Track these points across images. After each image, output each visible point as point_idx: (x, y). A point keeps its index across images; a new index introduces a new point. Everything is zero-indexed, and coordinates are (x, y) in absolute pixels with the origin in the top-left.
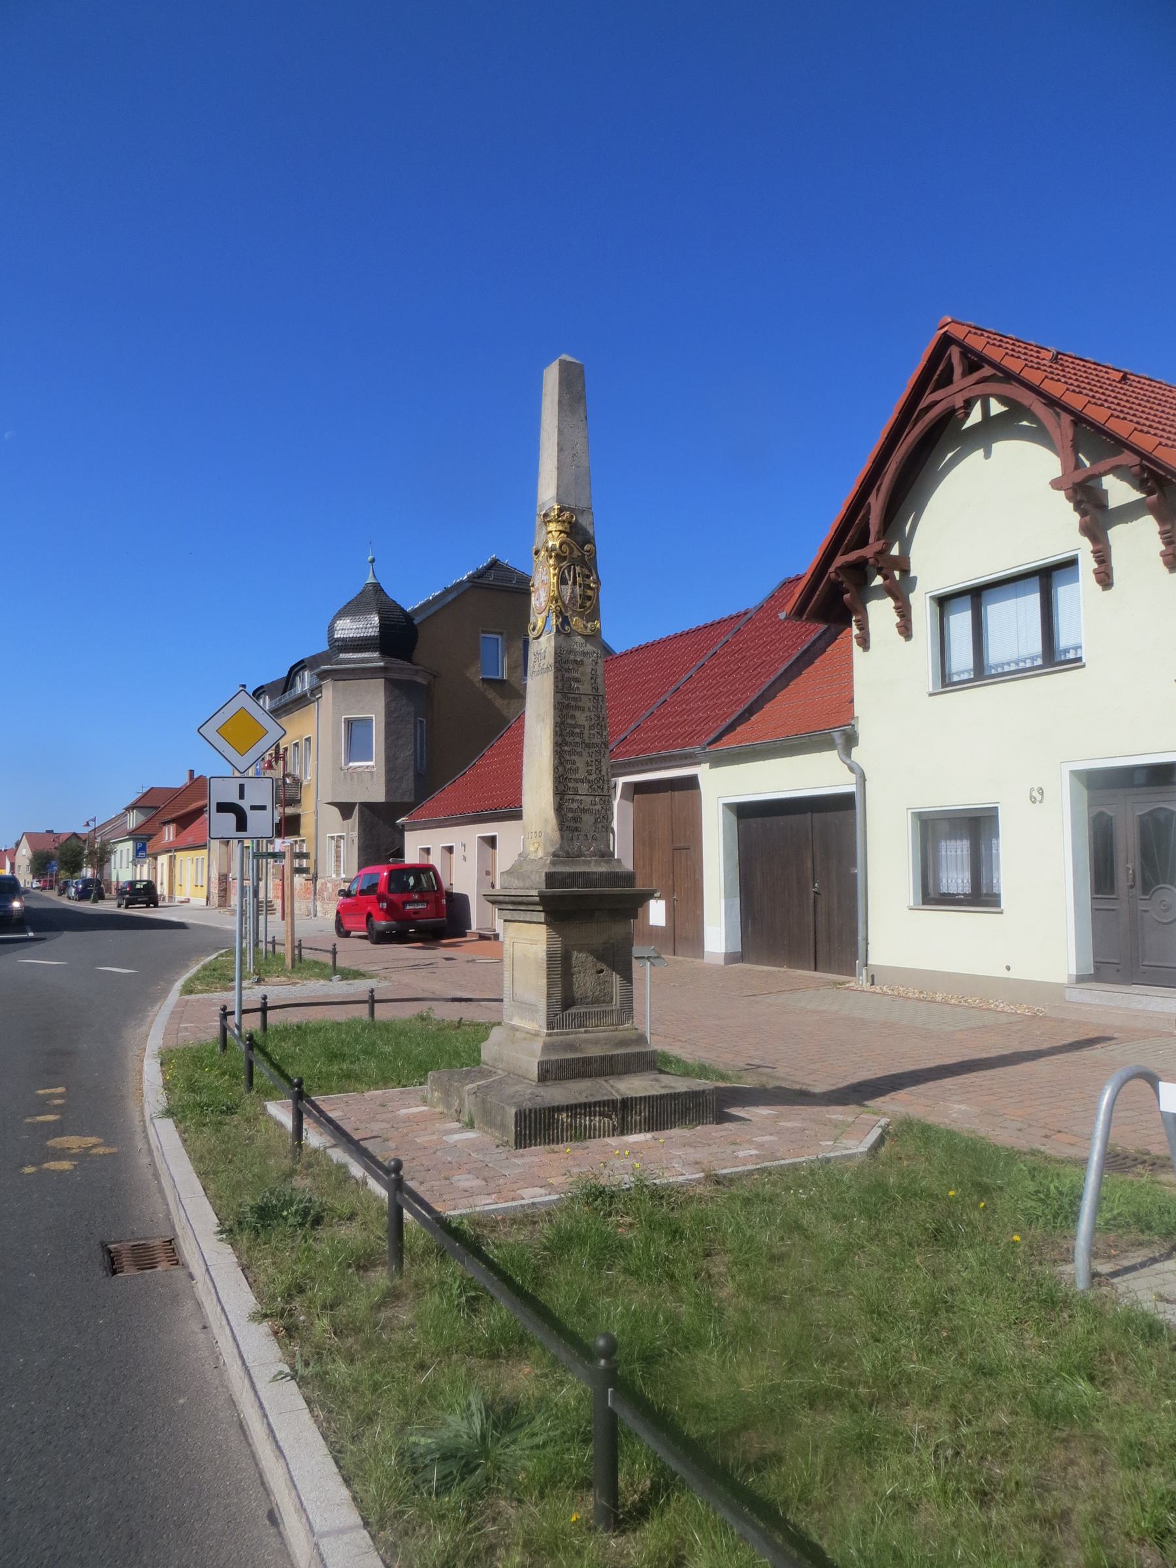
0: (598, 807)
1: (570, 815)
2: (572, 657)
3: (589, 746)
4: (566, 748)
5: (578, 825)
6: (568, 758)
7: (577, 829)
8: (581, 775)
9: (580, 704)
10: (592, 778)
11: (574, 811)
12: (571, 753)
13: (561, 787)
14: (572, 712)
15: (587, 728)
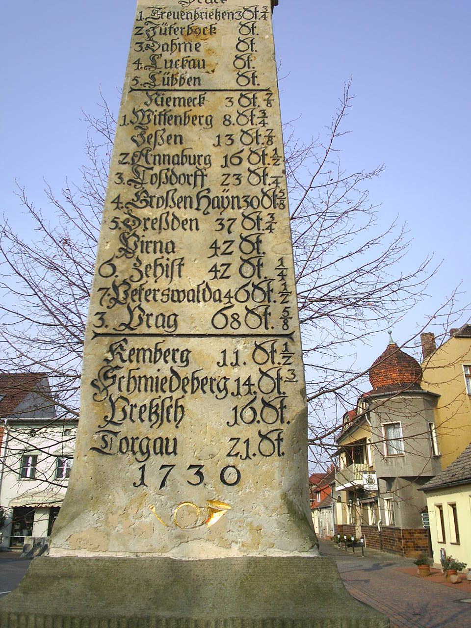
0: (250, 371)
1: (142, 398)
2: (184, 23)
3: (218, 204)
4: (147, 212)
5: (167, 431)
6: (150, 236)
7: (165, 447)
8: (190, 280)
9: (198, 111)
10: (224, 286)
11: (158, 384)
12: (159, 224)
13: (119, 316)
14: (172, 129)
15: (217, 161)
